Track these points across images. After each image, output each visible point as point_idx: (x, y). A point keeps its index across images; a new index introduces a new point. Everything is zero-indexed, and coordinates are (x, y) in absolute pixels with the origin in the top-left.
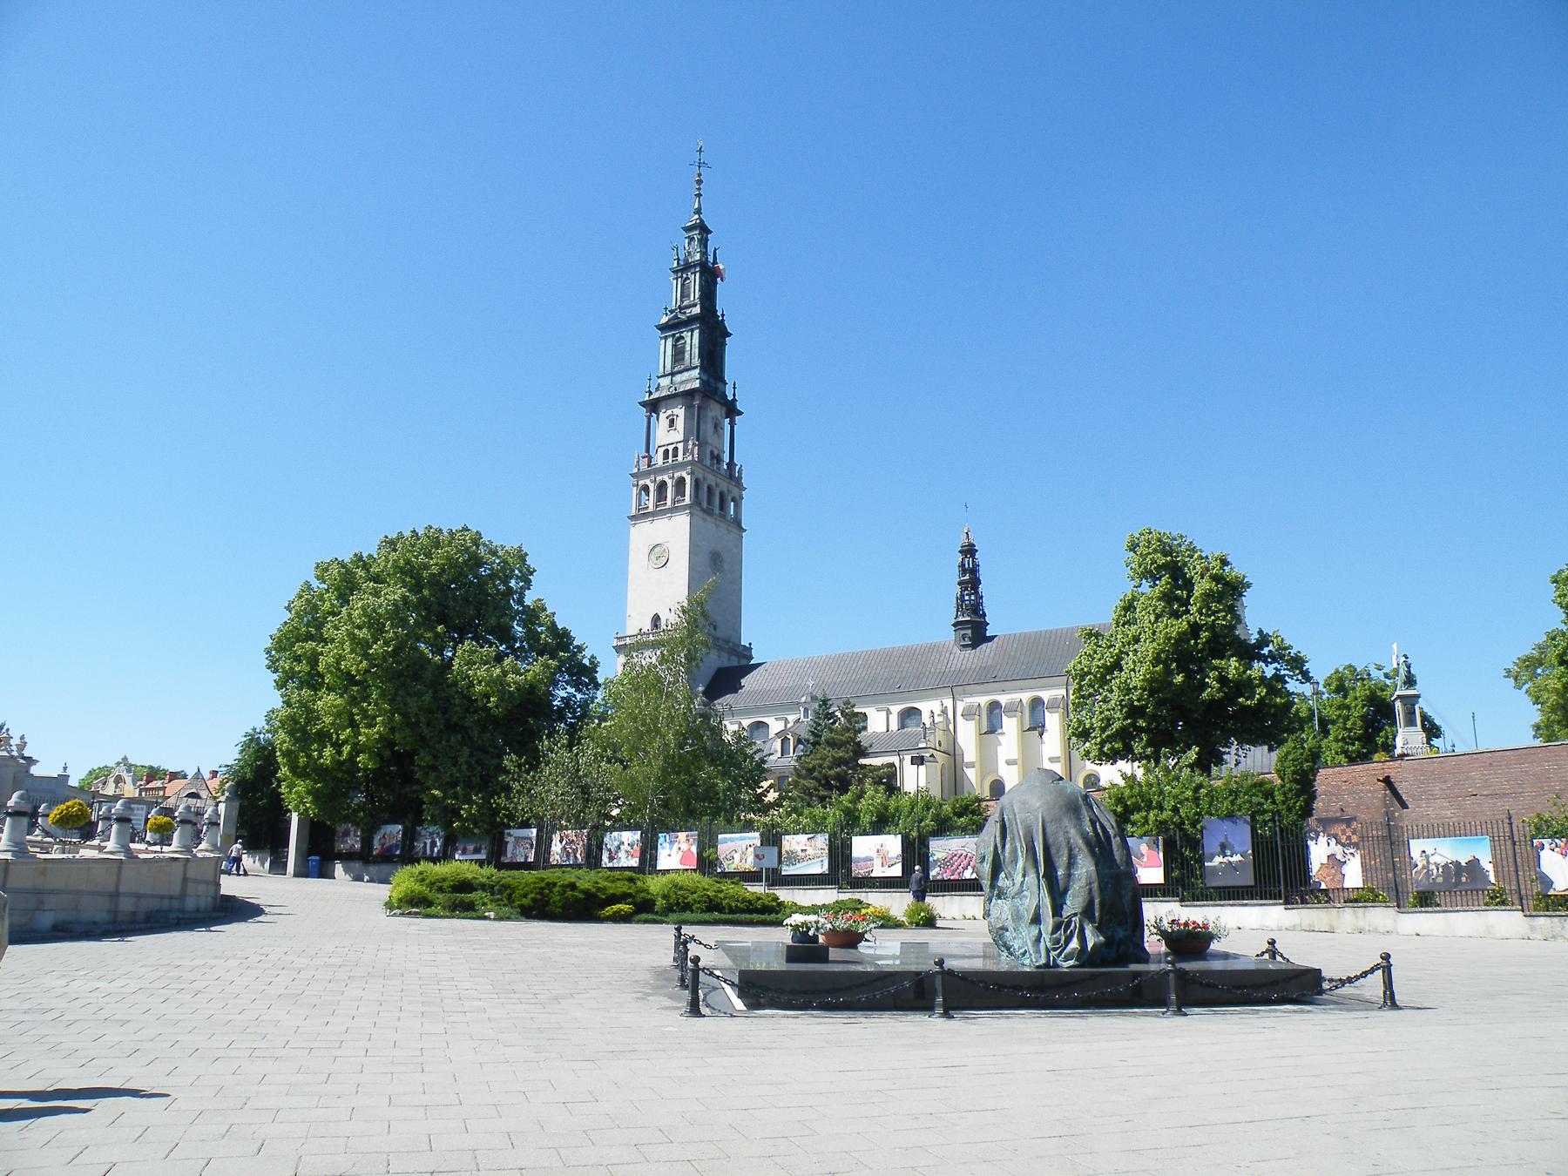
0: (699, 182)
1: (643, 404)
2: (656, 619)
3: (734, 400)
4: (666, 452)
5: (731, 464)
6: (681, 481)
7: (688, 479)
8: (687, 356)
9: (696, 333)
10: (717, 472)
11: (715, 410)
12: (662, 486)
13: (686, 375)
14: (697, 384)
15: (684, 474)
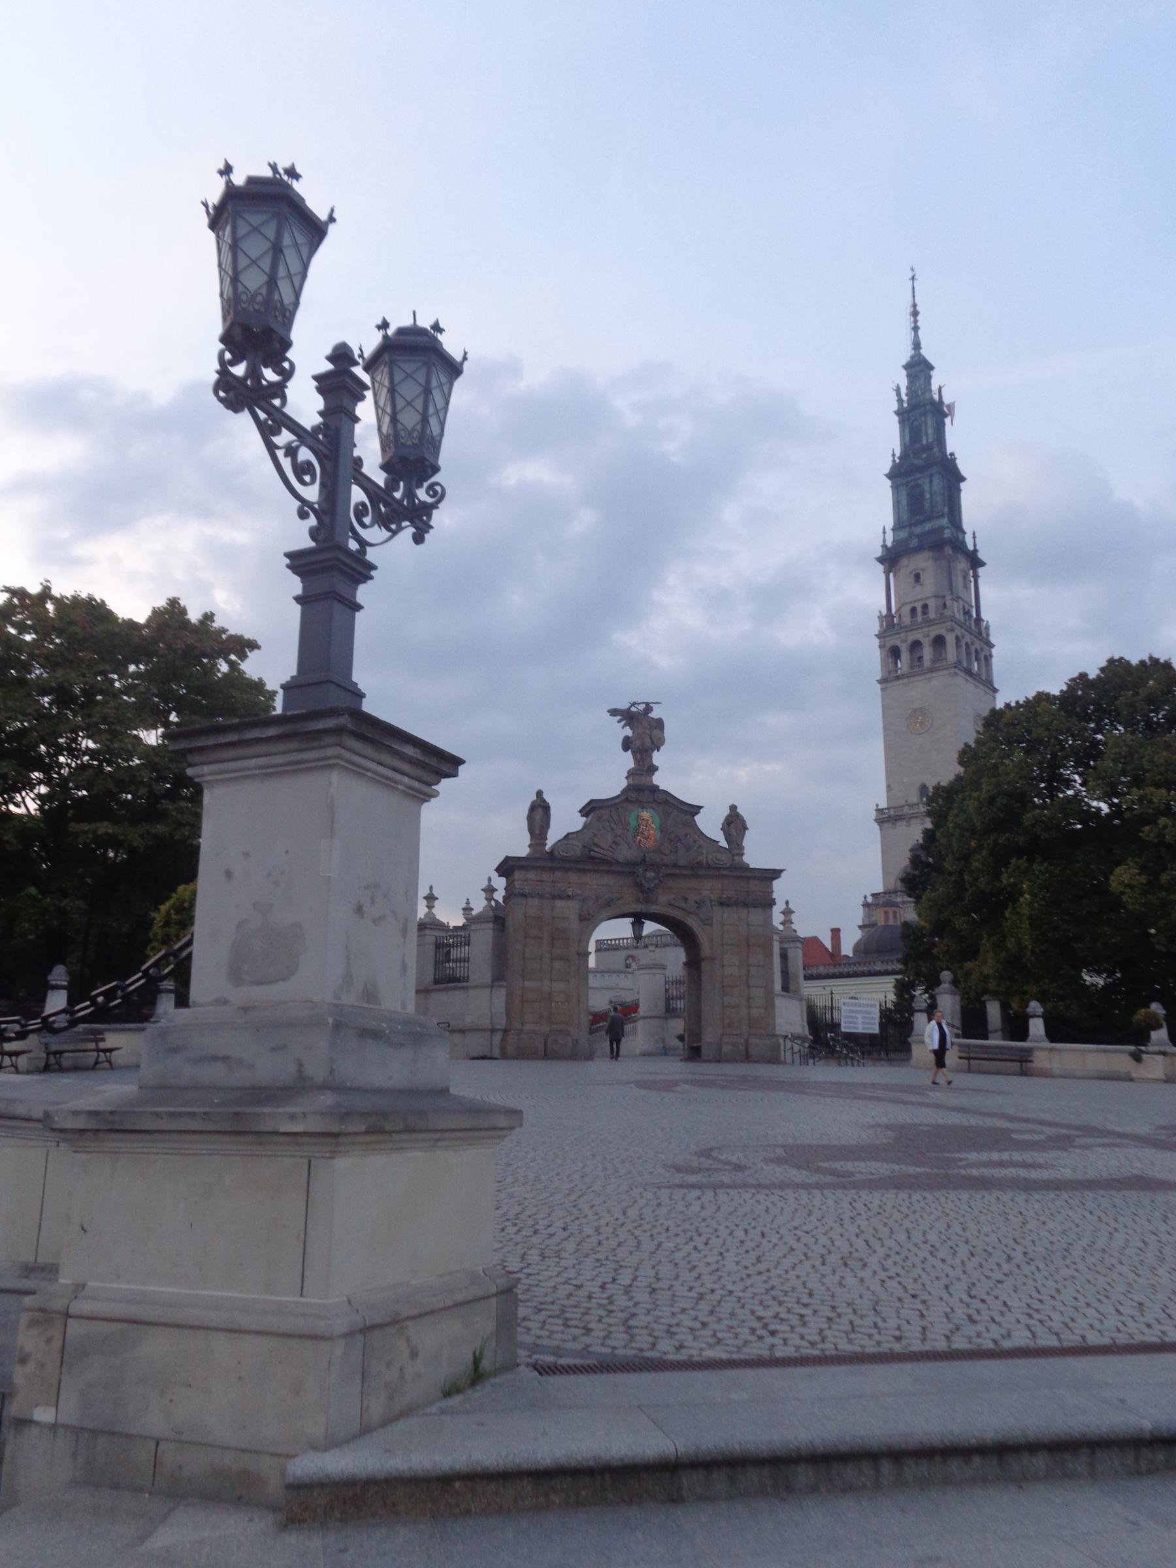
0: (915, 314)
1: (880, 560)
3: (976, 551)
4: (913, 610)
5: (979, 620)
6: (939, 641)
7: (950, 639)
8: (927, 505)
9: (936, 481)
10: (969, 630)
11: (962, 564)
12: (916, 645)
13: (928, 526)
14: (947, 534)
15: (943, 632)
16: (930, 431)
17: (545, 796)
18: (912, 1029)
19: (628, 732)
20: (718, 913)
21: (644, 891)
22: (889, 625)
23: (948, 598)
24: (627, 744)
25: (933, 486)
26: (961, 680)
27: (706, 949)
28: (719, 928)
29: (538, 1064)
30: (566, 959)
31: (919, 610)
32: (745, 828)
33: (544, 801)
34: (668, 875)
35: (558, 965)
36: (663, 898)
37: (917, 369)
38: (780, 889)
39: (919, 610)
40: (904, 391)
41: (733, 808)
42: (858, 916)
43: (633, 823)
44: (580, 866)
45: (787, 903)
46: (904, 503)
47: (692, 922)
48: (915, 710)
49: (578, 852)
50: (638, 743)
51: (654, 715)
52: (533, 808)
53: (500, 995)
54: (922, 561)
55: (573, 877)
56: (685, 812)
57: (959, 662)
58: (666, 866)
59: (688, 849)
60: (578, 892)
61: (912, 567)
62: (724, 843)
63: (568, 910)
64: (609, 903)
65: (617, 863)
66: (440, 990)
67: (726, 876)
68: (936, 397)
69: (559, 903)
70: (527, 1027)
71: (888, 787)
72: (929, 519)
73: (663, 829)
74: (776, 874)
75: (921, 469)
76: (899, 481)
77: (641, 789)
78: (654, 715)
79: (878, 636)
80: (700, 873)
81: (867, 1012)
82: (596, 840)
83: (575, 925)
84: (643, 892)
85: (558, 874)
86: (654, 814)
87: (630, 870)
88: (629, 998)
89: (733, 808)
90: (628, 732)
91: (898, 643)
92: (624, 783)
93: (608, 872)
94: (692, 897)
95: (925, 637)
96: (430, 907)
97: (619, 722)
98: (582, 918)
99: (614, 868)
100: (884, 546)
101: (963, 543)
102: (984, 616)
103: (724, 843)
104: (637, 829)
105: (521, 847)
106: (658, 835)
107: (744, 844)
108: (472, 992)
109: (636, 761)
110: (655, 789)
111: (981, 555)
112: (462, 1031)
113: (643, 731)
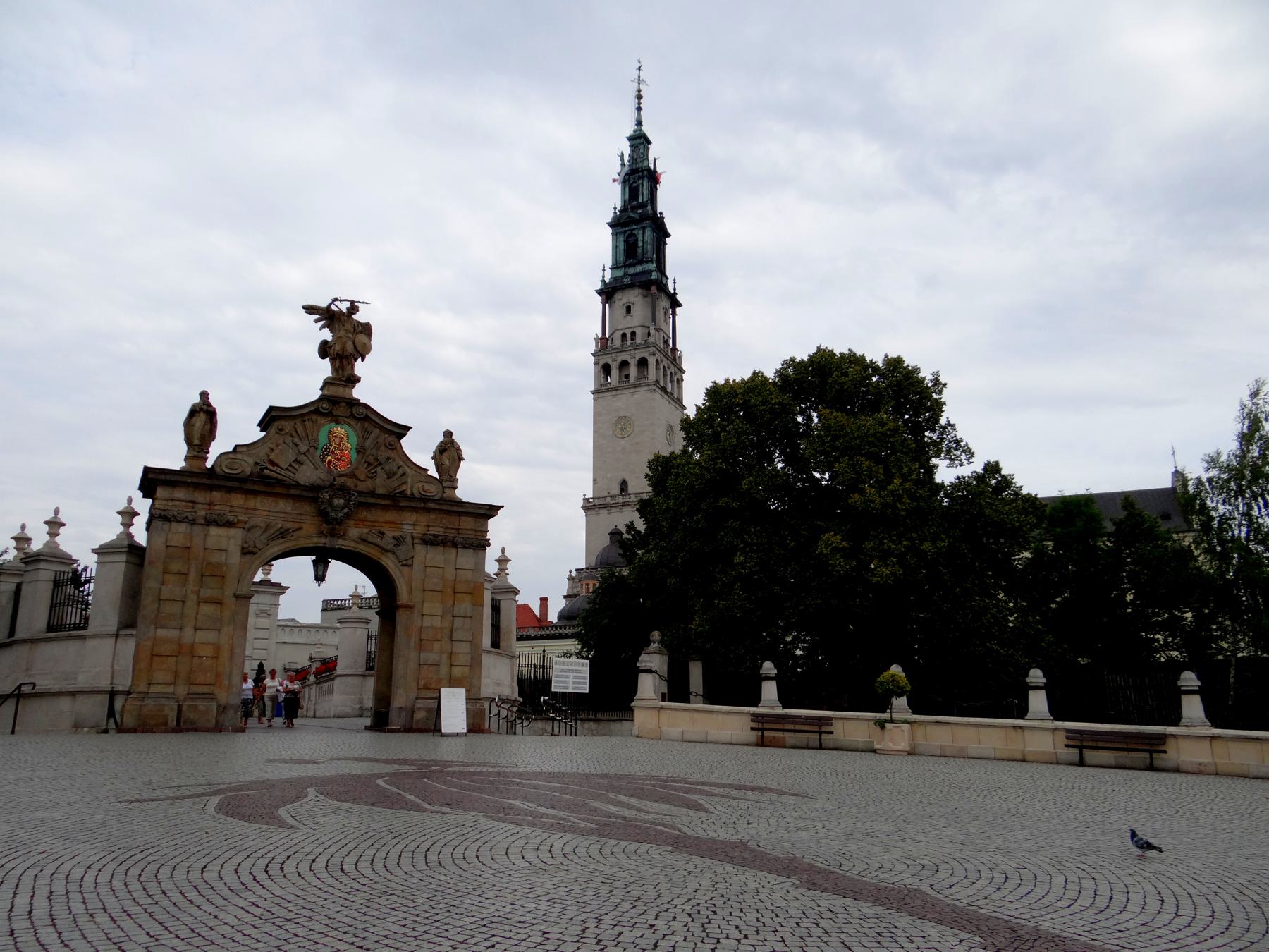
0: (639, 97)
1: (600, 292)
2: (624, 485)
3: (675, 294)
4: (624, 335)
5: (674, 349)
6: (643, 363)
7: (652, 361)
8: (639, 251)
9: (648, 232)
10: (666, 356)
11: (664, 303)
12: (624, 364)
13: (639, 268)
14: (654, 276)
15: (646, 355)
16: (646, 192)
17: (212, 400)
18: (636, 692)
19: (327, 335)
20: (422, 554)
21: (332, 525)
22: (603, 345)
23: (652, 328)
24: (324, 350)
25: (645, 237)
26: (658, 395)
27: (403, 597)
28: (423, 571)
29: (173, 735)
30: (219, 602)
31: (628, 336)
32: (460, 459)
33: (210, 405)
34: (362, 505)
35: (206, 609)
36: (354, 532)
37: (638, 141)
38: (496, 529)
39: (628, 336)
40: (626, 158)
41: (448, 434)
42: (564, 588)
43: (323, 440)
44: (248, 486)
45: (503, 550)
46: (622, 247)
47: (388, 562)
48: (621, 418)
49: (248, 471)
50: (337, 348)
51: (359, 317)
52: (193, 412)
53: (128, 647)
54: (634, 297)
55: (238, 500)
56: (391, 433)
57: (657, 381)
58: (361, 493)
59: (390, 475)
60: (242, 518)
61: (624, 300)
62: (433, 472)
63: (227, 541)
64: (283, 534)
65: (298, 485)
66: (57, 639)
67: (434, 510)
68: (652, 166)
69: (214, 531)
70: (154, 689)
71: (595, 480)
72: (641, 262)
73: (360, 450)
74: (492, 510)
75: (637, 222)
76: (618, 229)
77: (338, 402)
78: (359, 317)
79: (594, 355)
80: (402, 504)
81: (578, 671)
82: (272, 456)
83: (235, 558)
84: (328, 523)
85: (217, 495)
86: (349, 429)
87: (309, 494)
88: (329, 653)
89: (448, 434)
90: (327, 335)
91: (609, 361)
92: (315, 394)
93: (287, 497)
94: (390, 533)
95: (632, 358)
96: (53, 534)
97: (317, 321)
98: (245, 552)
99: (292, 491)
100: (603, 281)
101: (666, 286)
102: (678, 347)
103: (433, 472)
104: (326, 449)
105: (173, 457)
106: (354, 455)
107: (460, 475)
108: (91, 643)
109: (335, 369)
110: (356, 403)
111: (678, 297)
112: (73, 694)
113: (345, 336)
